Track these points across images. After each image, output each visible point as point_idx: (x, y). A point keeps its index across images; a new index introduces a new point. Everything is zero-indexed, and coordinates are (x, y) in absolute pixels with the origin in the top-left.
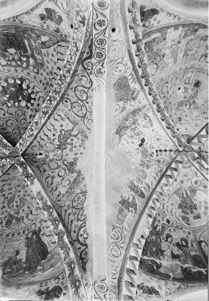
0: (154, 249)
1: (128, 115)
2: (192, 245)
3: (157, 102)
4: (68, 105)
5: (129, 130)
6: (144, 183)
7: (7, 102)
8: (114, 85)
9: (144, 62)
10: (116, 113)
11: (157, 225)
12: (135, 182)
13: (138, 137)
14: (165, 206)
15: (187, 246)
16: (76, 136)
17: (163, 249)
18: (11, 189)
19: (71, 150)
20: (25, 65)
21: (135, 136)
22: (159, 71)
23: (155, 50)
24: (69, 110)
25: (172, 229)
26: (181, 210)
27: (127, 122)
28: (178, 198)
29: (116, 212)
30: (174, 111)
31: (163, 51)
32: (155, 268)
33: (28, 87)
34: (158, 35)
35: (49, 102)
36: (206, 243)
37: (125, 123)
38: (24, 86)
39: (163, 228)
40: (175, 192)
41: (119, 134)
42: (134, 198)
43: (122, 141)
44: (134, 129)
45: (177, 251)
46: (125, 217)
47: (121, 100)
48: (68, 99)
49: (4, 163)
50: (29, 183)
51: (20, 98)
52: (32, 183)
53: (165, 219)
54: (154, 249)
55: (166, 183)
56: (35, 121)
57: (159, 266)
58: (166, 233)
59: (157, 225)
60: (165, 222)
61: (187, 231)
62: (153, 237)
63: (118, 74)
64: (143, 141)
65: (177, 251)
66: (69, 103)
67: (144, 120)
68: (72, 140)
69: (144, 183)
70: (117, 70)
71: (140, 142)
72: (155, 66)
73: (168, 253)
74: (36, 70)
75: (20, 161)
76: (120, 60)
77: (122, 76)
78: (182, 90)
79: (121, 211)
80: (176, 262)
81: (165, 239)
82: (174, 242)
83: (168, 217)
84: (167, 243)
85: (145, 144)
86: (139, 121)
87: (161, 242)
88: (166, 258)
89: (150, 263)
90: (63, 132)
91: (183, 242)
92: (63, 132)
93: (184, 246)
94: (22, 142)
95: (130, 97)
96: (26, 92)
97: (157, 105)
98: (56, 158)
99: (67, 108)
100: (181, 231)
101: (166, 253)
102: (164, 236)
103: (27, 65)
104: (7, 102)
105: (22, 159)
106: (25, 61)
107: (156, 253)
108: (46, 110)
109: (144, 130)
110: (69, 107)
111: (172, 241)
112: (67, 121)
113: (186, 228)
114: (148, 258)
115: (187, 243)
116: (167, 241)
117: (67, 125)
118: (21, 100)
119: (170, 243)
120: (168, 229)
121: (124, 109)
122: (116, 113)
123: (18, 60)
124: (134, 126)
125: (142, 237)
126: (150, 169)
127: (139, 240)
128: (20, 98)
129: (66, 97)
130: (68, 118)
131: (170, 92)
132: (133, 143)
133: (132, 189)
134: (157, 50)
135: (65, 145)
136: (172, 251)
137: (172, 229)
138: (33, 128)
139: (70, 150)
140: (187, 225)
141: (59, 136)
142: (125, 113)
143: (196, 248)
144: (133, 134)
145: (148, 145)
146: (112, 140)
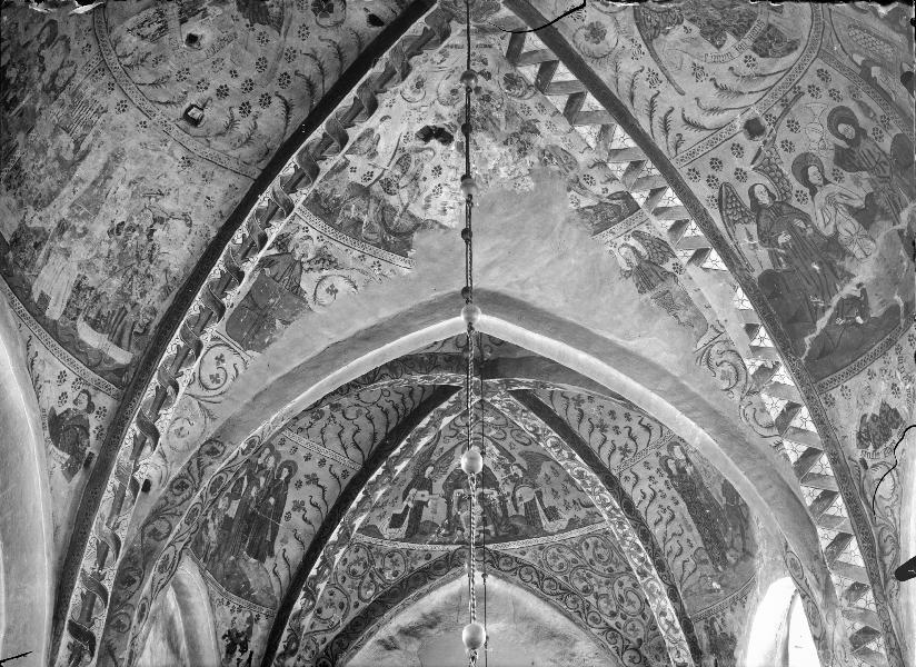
0: (816, 267)
1: (339, 228)
2: (866, 110)
3: (282, 196)
5: (393, 200)
6: (592, 173)
8: (261, 347)
9: (182, 344)
10: (342, 285)
11: (751, 193)
12: (585, 203)
13: (414, 157)
14: (694, 114)
15: (861, 132)
17: (829, 231)
21: (412, 168)
22: (167, 204)
23: (116, 282)
25: (784, 133)
26: (731, 40)
27: (365, 219)
28: (677, 33)
29: (665, 319)
30: (293, 41)
31: (105, 248)
32: (859, 320)
34: (91, 338)
36: (877, 65)
37: (370, 227)
39: (767, 167)
40: (648, 42)
41: (410, 233)
42: (637, 235)
43: (433, 214)
44: (388, 186)
45: (856, 189)
46: (689, 302)
47: (296, 291)
53: (742, 138)
54: (816, 267)
55: (597, 129)
57: (858, 303)
58: (786, 169)
59: (751, 193)
60: (751, 147)
61: (811, 78)
62: (782, 239)
63: (231, 360)
64: (428, 134)
65: (856, 189)
67: (351, 165)
69: (592, 173)
70: (221, 372)
71: (434, 143)
72: (159, 232)
73: (848, 227)
76: (195, 389)
77: (231, 342)
78: (194, 27)
79: (668, 303)
80: (885, 228)
81: (807, 191)
82: (827, 158)
83: (739, 124)
84: (821, 195)
85: (439, 124)
86: (356, 178)
87: (806, 218)
88: (855, 249)
89: (840, 321)
91: (841, 128)
93: (854, 143)
95: (280, 267)
97: (293, 190)
100: (802, 100)
101: (844, 235)
102: (796, 185)
107: (828, 271)
109: (385, 147)
111: (821, 170)
113: (800, 68)
114: (829, 313)
115: (852, 121)
116: (813, 192)
119: (826, 182)
120: (781, 151)
121: (325, 259)
122: (342, 285)
124: (377, 188)
125: (751, 329)
126: (543, 128)
127: (756, 350)
131: (215, 83)
132: (438, 170)
133: (605, 225)
134: (112, 274)
136: (850, 208)
137: (784, 133)
140: (793, 56)
142: (335, 249)
143: (879, 111)
144: (403, 182)
145: (445, 111)
146: (434, 260)
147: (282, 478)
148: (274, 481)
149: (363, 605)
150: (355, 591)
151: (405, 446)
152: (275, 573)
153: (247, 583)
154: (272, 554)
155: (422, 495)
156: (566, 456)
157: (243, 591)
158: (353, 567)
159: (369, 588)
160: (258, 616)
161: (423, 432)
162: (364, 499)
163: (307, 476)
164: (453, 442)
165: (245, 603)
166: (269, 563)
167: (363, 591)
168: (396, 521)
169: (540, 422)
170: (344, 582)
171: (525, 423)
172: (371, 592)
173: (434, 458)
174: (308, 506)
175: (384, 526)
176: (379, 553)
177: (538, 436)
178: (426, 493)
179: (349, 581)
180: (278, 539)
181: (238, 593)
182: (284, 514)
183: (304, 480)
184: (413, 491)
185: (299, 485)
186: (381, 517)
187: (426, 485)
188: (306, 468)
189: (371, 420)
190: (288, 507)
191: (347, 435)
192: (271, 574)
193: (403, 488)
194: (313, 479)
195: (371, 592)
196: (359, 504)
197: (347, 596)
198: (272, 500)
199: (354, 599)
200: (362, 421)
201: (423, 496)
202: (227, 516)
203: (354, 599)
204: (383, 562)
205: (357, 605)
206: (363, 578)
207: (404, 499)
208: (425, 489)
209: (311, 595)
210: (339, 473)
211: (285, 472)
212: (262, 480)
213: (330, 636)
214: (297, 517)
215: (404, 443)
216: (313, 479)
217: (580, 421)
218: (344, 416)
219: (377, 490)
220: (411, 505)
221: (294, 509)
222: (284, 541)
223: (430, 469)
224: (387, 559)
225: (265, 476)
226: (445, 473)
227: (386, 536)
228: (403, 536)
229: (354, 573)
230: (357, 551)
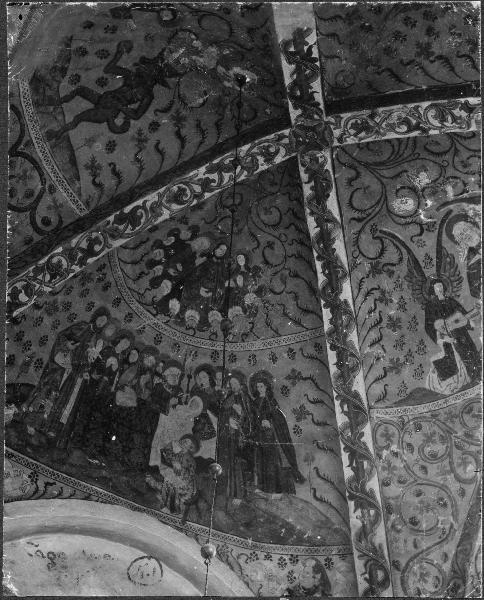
4: (49, 208)
7: (243, 269)
16: (83, 92)
18: (397, 35)
19: (126, 46)
20: (123, 345)
24: (52, 189)
33: (155, 283)
35: (97, 248)
38: (166, 287)
48: (37, 229)
49: (352, 132)
50: (312, 39)
51: (199, 261)
52: (300, 35)
56: (175, 207)
66: (42, 211)
68: (101, 82)
74: (101, 321)
75: (305, 110)
90: (119, 121)
92: (119, 121)
94: (261, 159)
96: (171, 272)
98: (197, 43)
99: (54, 201)
103: (115, 343)
104: (243, 269)
105: (294, 114)
106: (115, 355)
108: (121, 227)
110: (47, 199)
112: (83, 156)
117: (90, 141)
118: (202, 256)
123: (130, 364)
128: (199, 261)
129: (37, 238)
130: (73, 161)
135: (139, 75)
138: (198, 189)
139: (129, 50)
141: (138, 114)
147: (263, 394)
148: (254, 404)
149: (470, 489)
150: (450, 477)
151: (323, 267)
152: (321, 500)
153: (286, 525)
154: (302, 480)
155: (456, 321)
156: (464, 114)
157: (279, 534)
158: (428, 449)
159: (465, 463)
160: (328, 560)
161: (325, 238)
162: (339, 356)
163: (288, 378)
164: (430, 240)
165: (292, 550)
166: (303, 492)
167: (459, 471)
168: (446, 369)
169: (398, 111)
170: (426, 472)
171: (392, 128)
172: (471, 468)
173: (430, 272)
174: (310, 407)
175: (431, 380)
176: (451, 416)
177: (417, 127)
178: (458, 315)
179: (433, 469)
180: (300, 461)
181: (280, 541)
182: (291, 431)
183: (287, 383)
184: (438, 324)
185: (285, 391)
186: (420, 373)
187: (450, 307)
188: (279, 372)
189: (296, 276)
190: (291, 423)
191: (292, 310)
192: (316, 503)
193: (421, 326)
194: (295, 377)
195: (471, 468)
196: (338, 365)
197: (443, 487)
198: (266, 423)
199: (454, 486)
200: (292, 284)
201: (457, 321)
202: (200, 459)
203: (454, 486)
204: (464, 424)
205: (463, 493)
206: (450, 455)
207: (434, 339)
208: (452, 312)
209: (365, 501)
210: (315, 353)
211: (262, 389)
212: (238, 408)
213: (451, 548)
214: (307, 426)
215: (318, 265)
216: (295, 377)
217: (452, 69)
218: (275, 293)
219: (346, 335)
220: (448, 339)
221: (298, 419)
222: (309, 459)
223: (438, 288)
224: (466, 417)
225: (238, 399)
226: (460, 280)
227: (447, 393)
228: (469, 379)
229: (434, 456)
230: (419, 428)
